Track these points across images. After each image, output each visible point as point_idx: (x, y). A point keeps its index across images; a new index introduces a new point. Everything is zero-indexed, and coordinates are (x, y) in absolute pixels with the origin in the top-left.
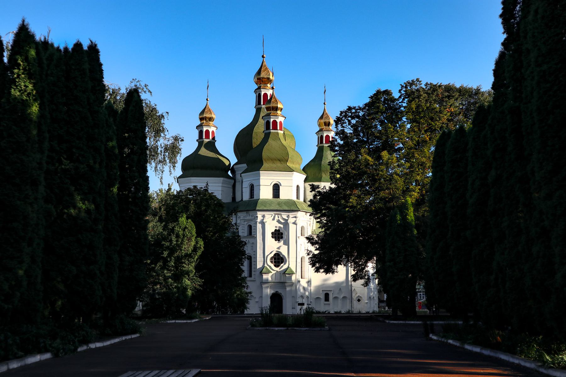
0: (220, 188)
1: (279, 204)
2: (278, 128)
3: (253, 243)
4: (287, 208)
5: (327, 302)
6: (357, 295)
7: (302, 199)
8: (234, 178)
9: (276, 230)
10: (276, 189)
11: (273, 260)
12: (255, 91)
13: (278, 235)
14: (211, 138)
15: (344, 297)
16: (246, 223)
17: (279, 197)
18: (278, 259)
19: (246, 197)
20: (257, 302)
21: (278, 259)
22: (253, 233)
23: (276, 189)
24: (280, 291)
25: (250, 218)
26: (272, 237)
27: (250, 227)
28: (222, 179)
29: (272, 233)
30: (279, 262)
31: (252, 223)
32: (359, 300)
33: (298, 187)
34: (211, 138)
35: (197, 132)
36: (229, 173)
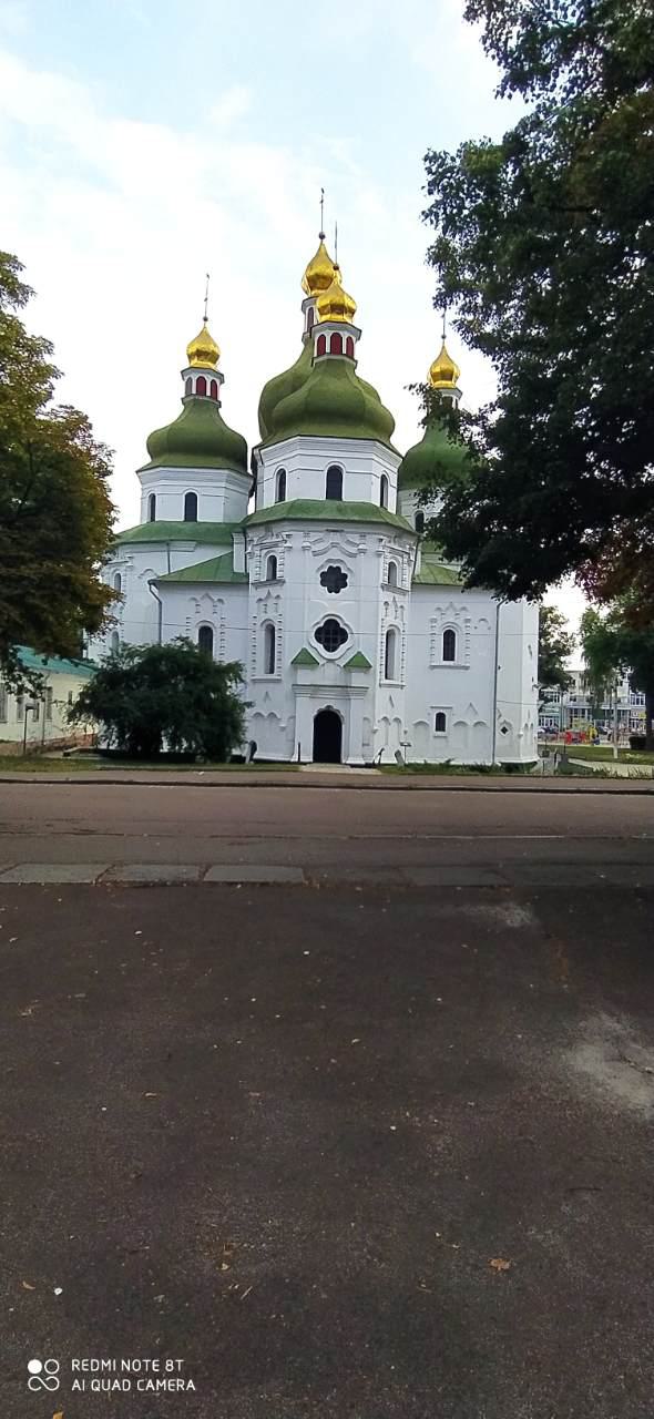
1: (340, 510)
2: (344, 351)
3: (278, 597)
4: (356, 518)
5: (440, 733)
6: (502, 720)
7: (392, 509)
8: (254, 477)
11: (323, 636)
12: (303, 310)
13: (334, 579)
14: (208, 393)
15: (479, 723)
17: (341, 499)
18: (332, 634)
19: (269, 496)
20: (283, 729)
21: (332, 634)
22: (278, 574)
23: (335, 476)
24: (336, 706)
25: (275, 539)
26: (323, 584)
27: (273, 561)
28: (226, 472)
30: (335, 641)
31: (277, 552)
32: (504, 730)
33: (384, 479)
34: (208, 393)
35: (182, 385)
36: (250, 471)
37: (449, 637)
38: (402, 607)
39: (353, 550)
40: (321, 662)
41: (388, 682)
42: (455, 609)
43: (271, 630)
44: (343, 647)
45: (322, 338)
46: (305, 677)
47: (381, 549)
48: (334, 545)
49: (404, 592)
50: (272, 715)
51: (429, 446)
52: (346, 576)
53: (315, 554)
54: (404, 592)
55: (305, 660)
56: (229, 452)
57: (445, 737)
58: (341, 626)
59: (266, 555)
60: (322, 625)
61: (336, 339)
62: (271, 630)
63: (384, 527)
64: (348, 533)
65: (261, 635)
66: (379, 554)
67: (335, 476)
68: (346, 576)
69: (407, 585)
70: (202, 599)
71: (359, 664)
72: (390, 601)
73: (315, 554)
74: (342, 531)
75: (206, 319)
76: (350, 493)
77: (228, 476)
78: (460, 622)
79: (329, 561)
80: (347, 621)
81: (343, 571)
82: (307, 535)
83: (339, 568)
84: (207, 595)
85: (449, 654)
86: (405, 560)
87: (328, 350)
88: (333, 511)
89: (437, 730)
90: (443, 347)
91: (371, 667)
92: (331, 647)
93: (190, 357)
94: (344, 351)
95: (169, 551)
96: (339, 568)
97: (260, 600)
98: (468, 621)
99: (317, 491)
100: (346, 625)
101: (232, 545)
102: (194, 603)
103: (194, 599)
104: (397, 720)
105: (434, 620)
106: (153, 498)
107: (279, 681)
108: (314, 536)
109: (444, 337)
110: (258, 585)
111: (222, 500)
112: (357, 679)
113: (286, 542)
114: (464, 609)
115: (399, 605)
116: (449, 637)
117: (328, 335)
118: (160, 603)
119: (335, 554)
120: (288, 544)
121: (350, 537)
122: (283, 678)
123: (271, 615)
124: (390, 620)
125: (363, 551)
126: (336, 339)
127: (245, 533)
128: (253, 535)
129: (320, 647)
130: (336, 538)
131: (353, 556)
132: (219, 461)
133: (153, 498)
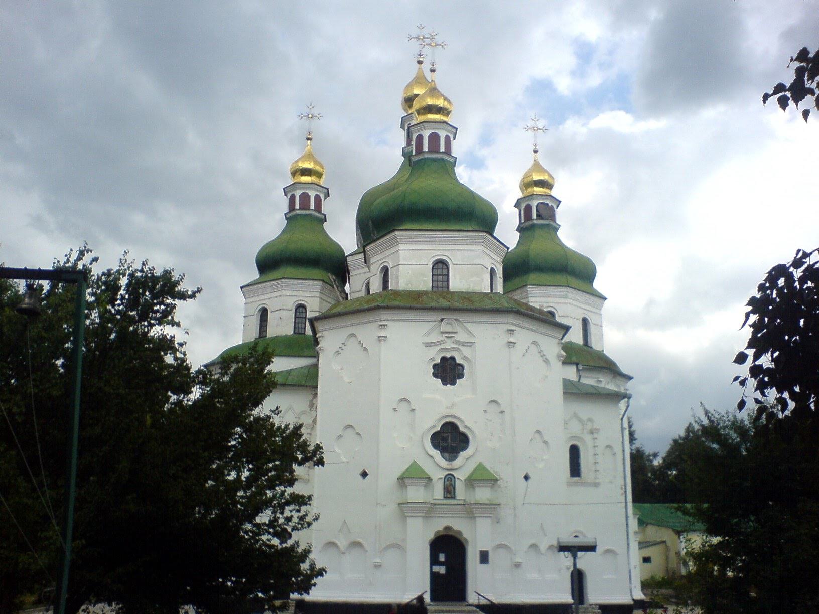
12: (402, 127)
21: (450, 439)
24: (459, 525)
44: (463, 455)
45: (420, 139)
58: (462, 429)
61: (434, 138)
67: (441, 267)
80: (468, 422)
88: (440, 300)
99: (425, 283)
100: (466, 427)
112: (482, 494)
117: (426, 134)
126: (434, 138)
129: (436, 454)
132: (317, 273)
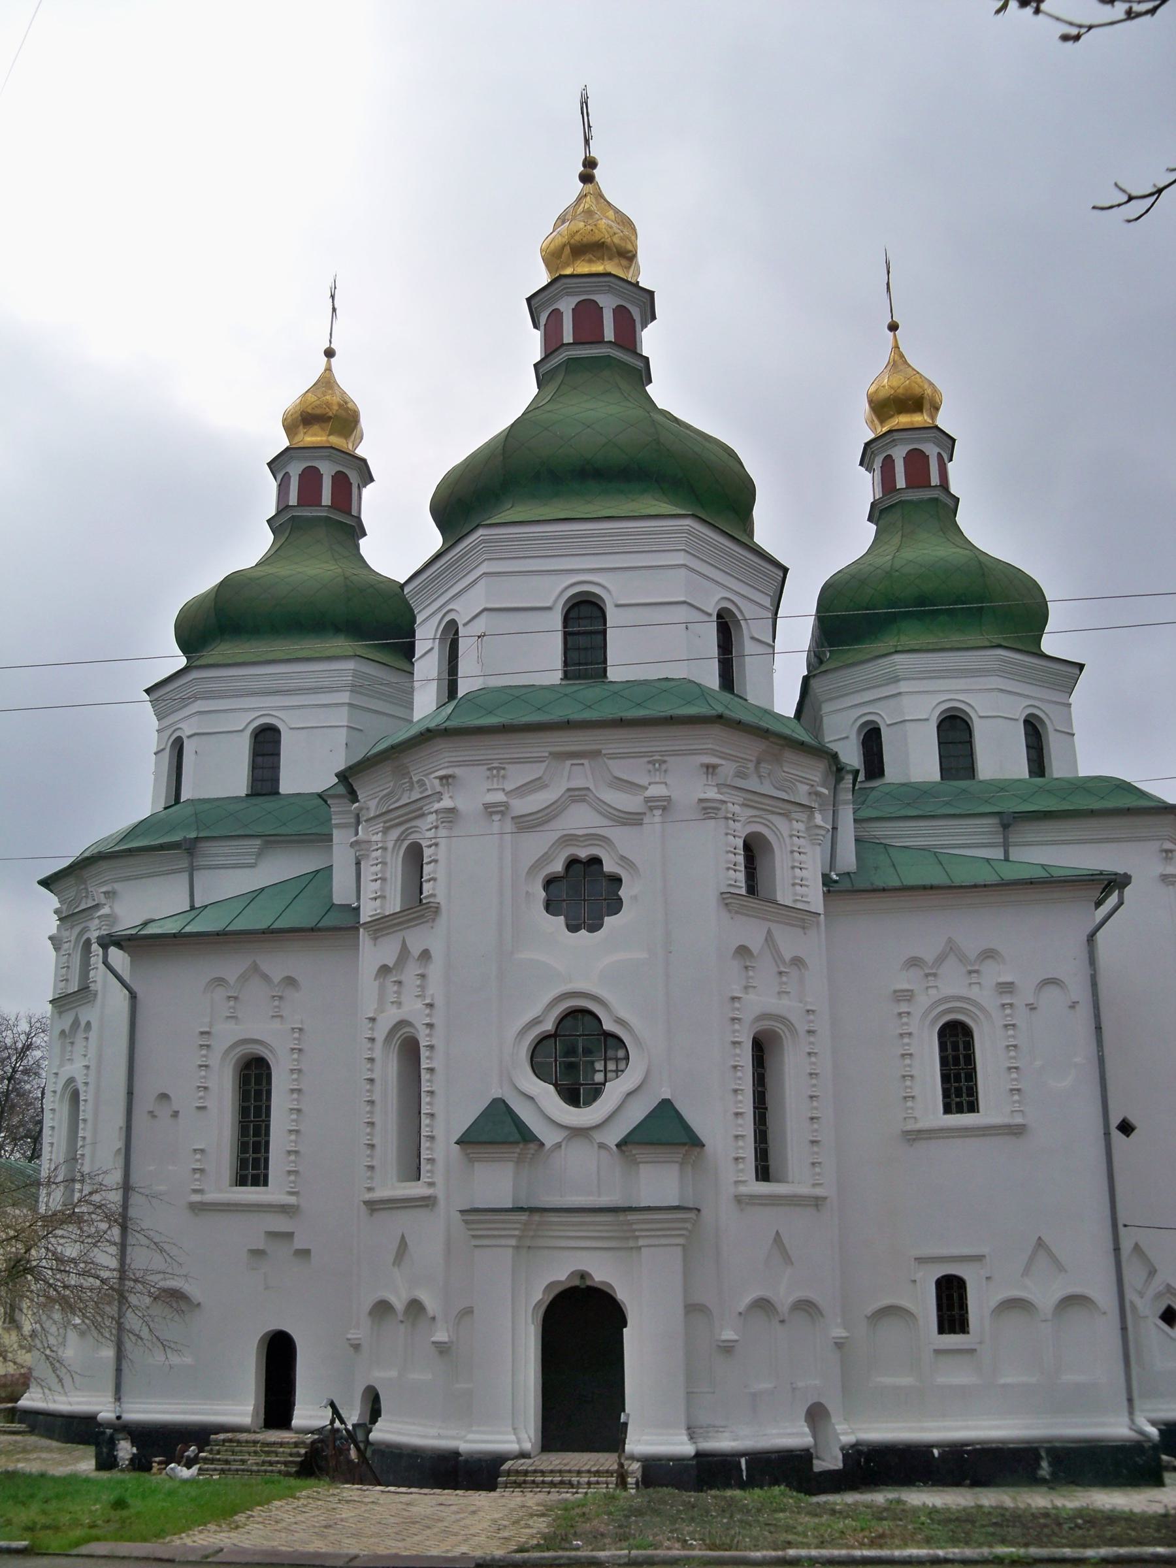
0: (341, 717)
2: (609, 334)
5: (953, 1340)
9: (572, 862)
10: (584, 620)
14: (326, 499)
15: (1071, 1301)
16: (394, 834)
19: (425, 703)
20: (443, 1349)
23: (584, 620)
25: (416, 795)
27: (415, 856)
28: (350, 665)
29: (549, 883)
31: (424, 831)
37: (956, 1043)
38: (797, 962)
39: (629, 802)
40: (549, 1137)
41: (764, 1188)
42: (962, 958)
43: (410, 1052)
44: (614, 1091)
46: (496, 1183)
47: (712, 794)
48: (577, 796)
49: (800, 918)
50: (415, 1307)
51: (884, 560)
52: (617, 880)
53: (526, 824)
54: (800, 918)
55: (499, 1131)
56: (380, 623)
57: (972, 1351)
59: (400, 840)
60: (549, 1026)
62: (410, 1051)
63: (716, 731)
64: (613, 756)
65: (389, 1068)
66: (708, 809)
68: (617, 880)
69: (815, 897)
70: (244, 978)
71: (665, 1132)
72: (756, 943)
73: (526, 824)
74: (595, 754)
75: (330, 353)
76: (628, 657)
77: (356, 674)
78: (985, 996)
79: (568, 839)
81: (609, 867)
82: (497, 771)
83: (596, 861)
84: (255, 968)
85: (960, 1089)
86: (801, 826)
87: (568, 337)
89: (941, 1331)
90: (897, 347)
91: (695, 1142)
92: (575, 1093)
93: (290, 427)
94: (609, 334)
95: (192, 871)
96: (596, 861)
97: (384, 970)
98: (1006, 988)
101: (328, 838)
102: (220, 993)
103: (220, 981)
104: (806, 1307)
105: (905, 996)
106: (178, 747)
107: (428, 1202)
108: (519, 775)
109: (893, 327)
110: (382, 926)
111: (342, 736)
113: (439, 796)
114: (989, 954)
115: (787, 956)
116: (956, 1043)
118: (133, 996)
119: (580, 820)
120: (446, 803)
121: (620, 769)
122: (439, 1191)
123: (412, 1009)
124: (764, 999)
125: (664, 805)
127: (353, 796)
128: (371, 796)
129: (546, 1094)
130: (580, 776)
131: (632, 820)
132: (341, 644)
133: (178, 747)
